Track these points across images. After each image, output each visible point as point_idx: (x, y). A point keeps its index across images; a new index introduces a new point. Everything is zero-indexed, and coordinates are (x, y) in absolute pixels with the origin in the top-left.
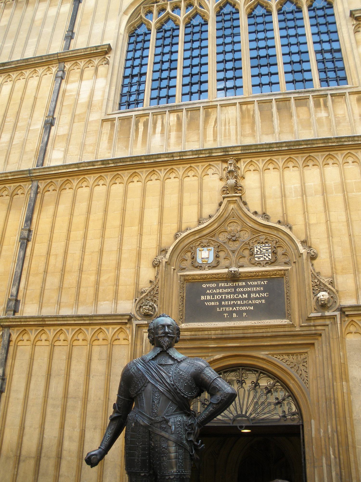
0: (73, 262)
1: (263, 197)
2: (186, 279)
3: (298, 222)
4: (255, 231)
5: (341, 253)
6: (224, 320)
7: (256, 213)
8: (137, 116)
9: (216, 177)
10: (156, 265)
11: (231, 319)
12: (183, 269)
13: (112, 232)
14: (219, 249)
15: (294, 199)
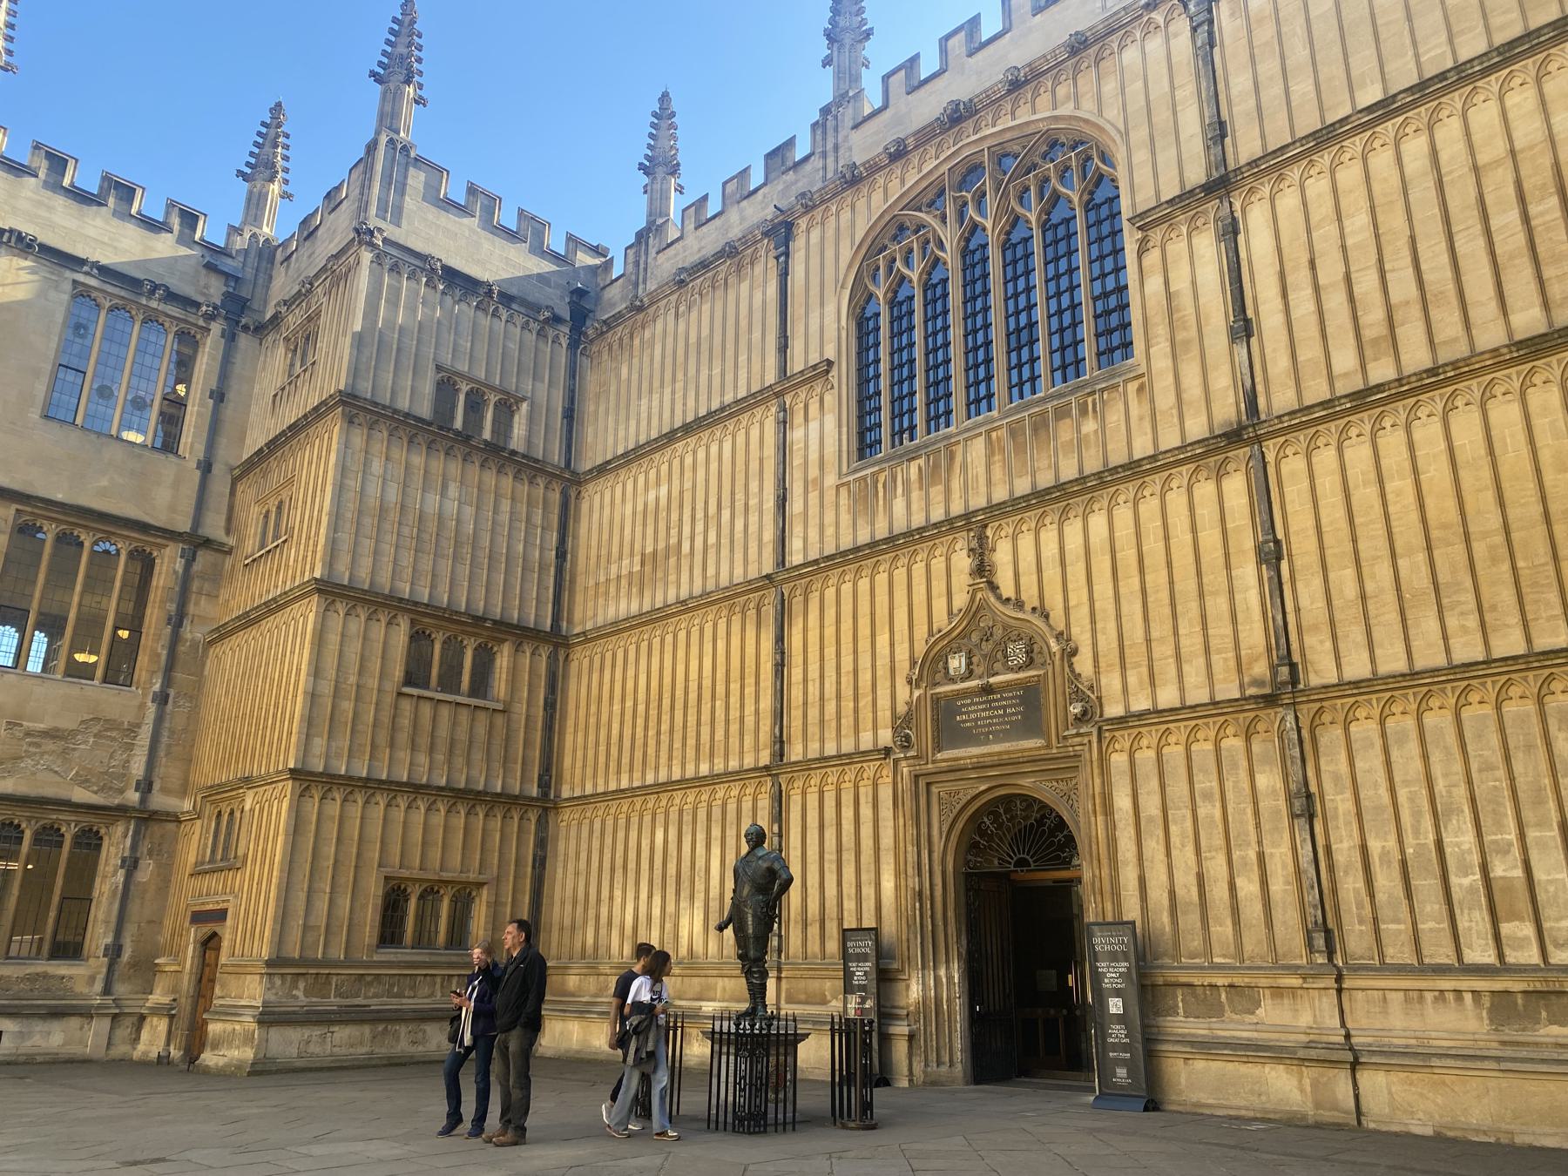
5: (1107, 641)
6: (979, 744)
8: (873, 474)
9: (965, 552)
11: (987, 742)
12: (936, 684)
15: (1052, 573)
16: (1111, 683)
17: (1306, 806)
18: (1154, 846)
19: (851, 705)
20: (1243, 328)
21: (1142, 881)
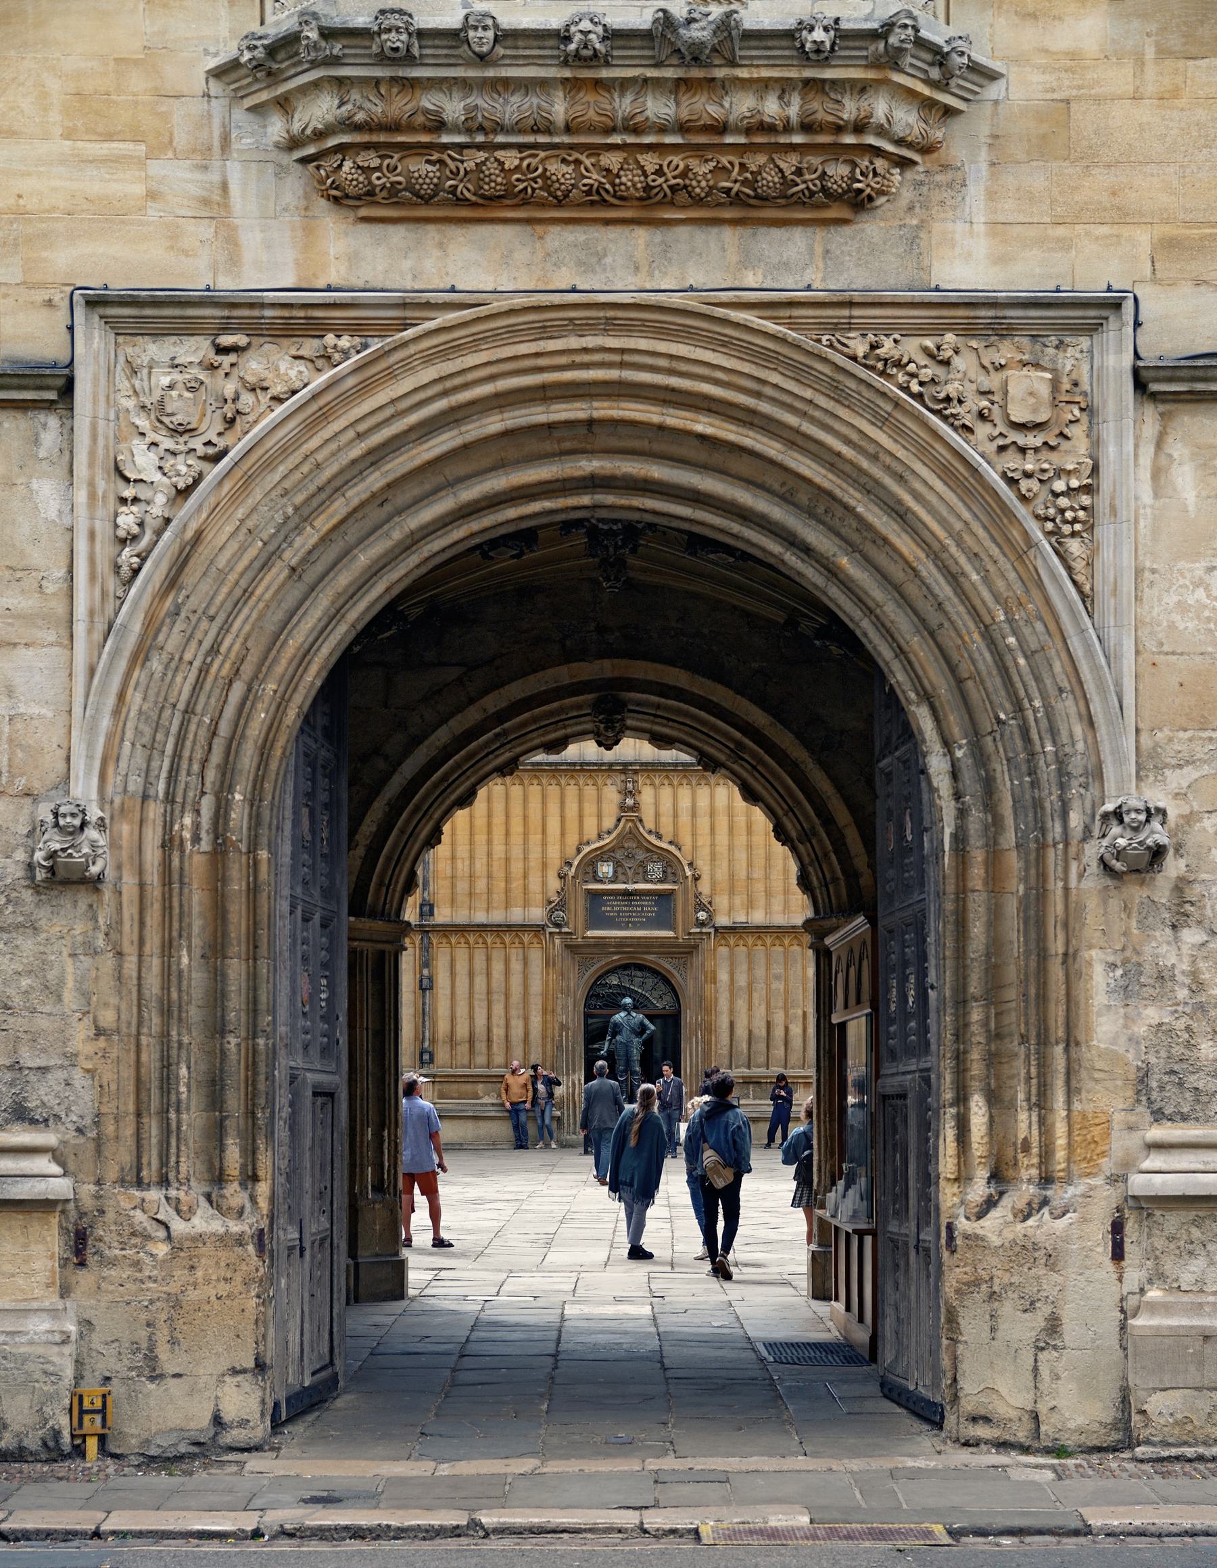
0: (480, 866)
1: (657, 815)
2: (589, 891)
3: (686, 840)
4: (648, 850)
5: (722, 874)
6: (620, 929)
7: (650, 832)
10: (562, 877)
11: (627, 928)
13: (516, 839)
14: (618, 864)
15: (685, 819)
16: (722, 902)
18: (741, 1004)
19: (503, 885)
21: (732, 1024)
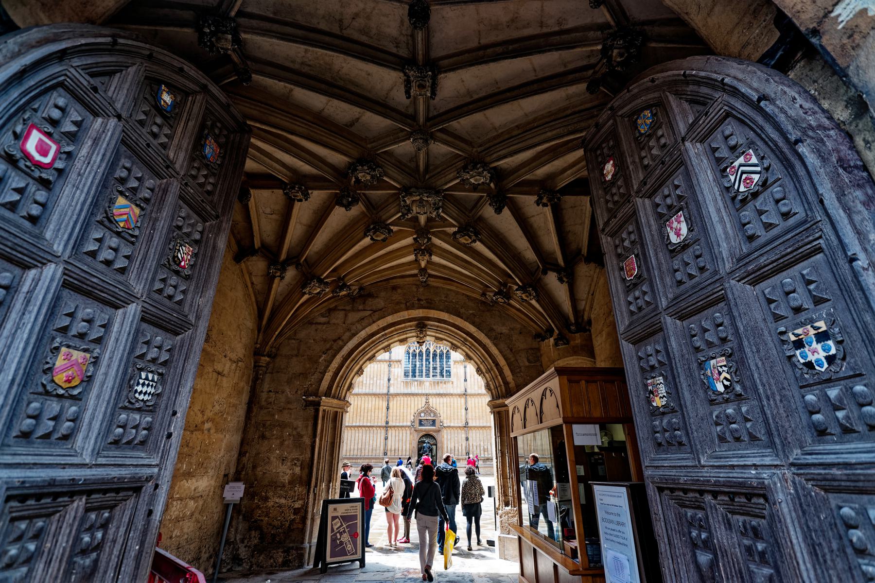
17: (467, 439)
20: (466, 380)
